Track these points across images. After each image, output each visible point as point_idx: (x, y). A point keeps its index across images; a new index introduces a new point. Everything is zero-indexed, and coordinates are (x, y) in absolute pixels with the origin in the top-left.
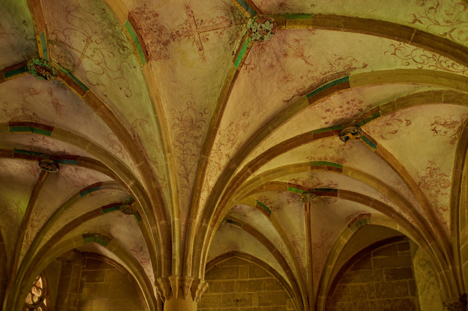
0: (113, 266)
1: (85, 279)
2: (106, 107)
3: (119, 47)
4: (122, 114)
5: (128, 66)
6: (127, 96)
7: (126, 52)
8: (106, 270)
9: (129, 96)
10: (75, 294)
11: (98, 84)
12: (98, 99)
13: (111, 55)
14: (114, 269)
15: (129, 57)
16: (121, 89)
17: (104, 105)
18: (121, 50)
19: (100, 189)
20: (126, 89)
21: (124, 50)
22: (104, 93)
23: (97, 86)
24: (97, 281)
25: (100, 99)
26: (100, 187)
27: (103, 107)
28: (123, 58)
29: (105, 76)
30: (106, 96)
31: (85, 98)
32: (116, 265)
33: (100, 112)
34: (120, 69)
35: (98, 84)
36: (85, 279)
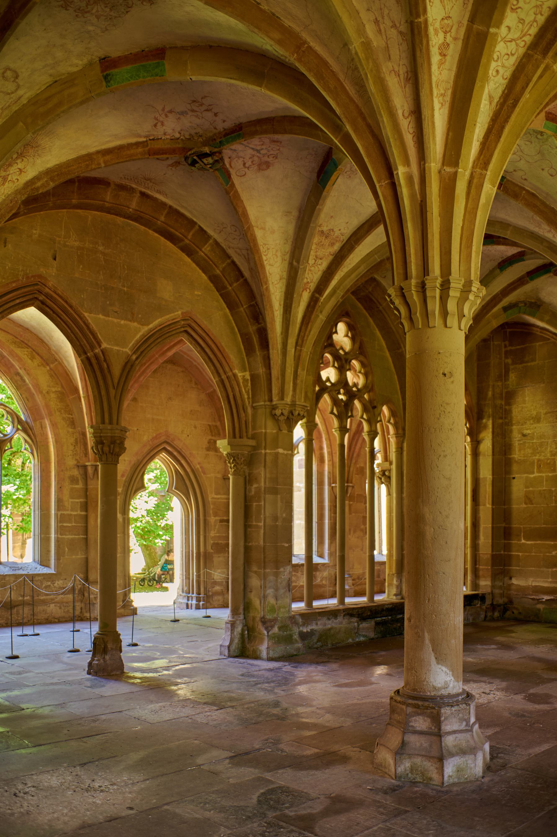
0: (546, 338)
1: (509, 361)
2: (527, 191)
3: (536, 134)
4: (547, 194)
5: (550, 148)
6: (552, 176)
7: (545, 137)
8: (538, 344)
9: (553, 174)
10: (500, 384)
11: (515, 171)
12: (517, 185)
13: (527, 143)
14: (549, 341)
15: (550, 140)
16: (543, 170)
17: (524, 189)
18: (539, 136)
19: (523, 260)
20: (548, 169)
21: (542, 135)
22: (524, 177)
23: (514, 173)
24: (527, 362)
25: (519, 184)
26: (524, 258)
27: (524, 192)
28: (543, 142)
29: (522, 162)
30: (525, 179)
31: (503, 191)
32: (551, 335)
33: (521, 200)
34: (540, 152)
35: (515, 171)
36: (509, 361)
